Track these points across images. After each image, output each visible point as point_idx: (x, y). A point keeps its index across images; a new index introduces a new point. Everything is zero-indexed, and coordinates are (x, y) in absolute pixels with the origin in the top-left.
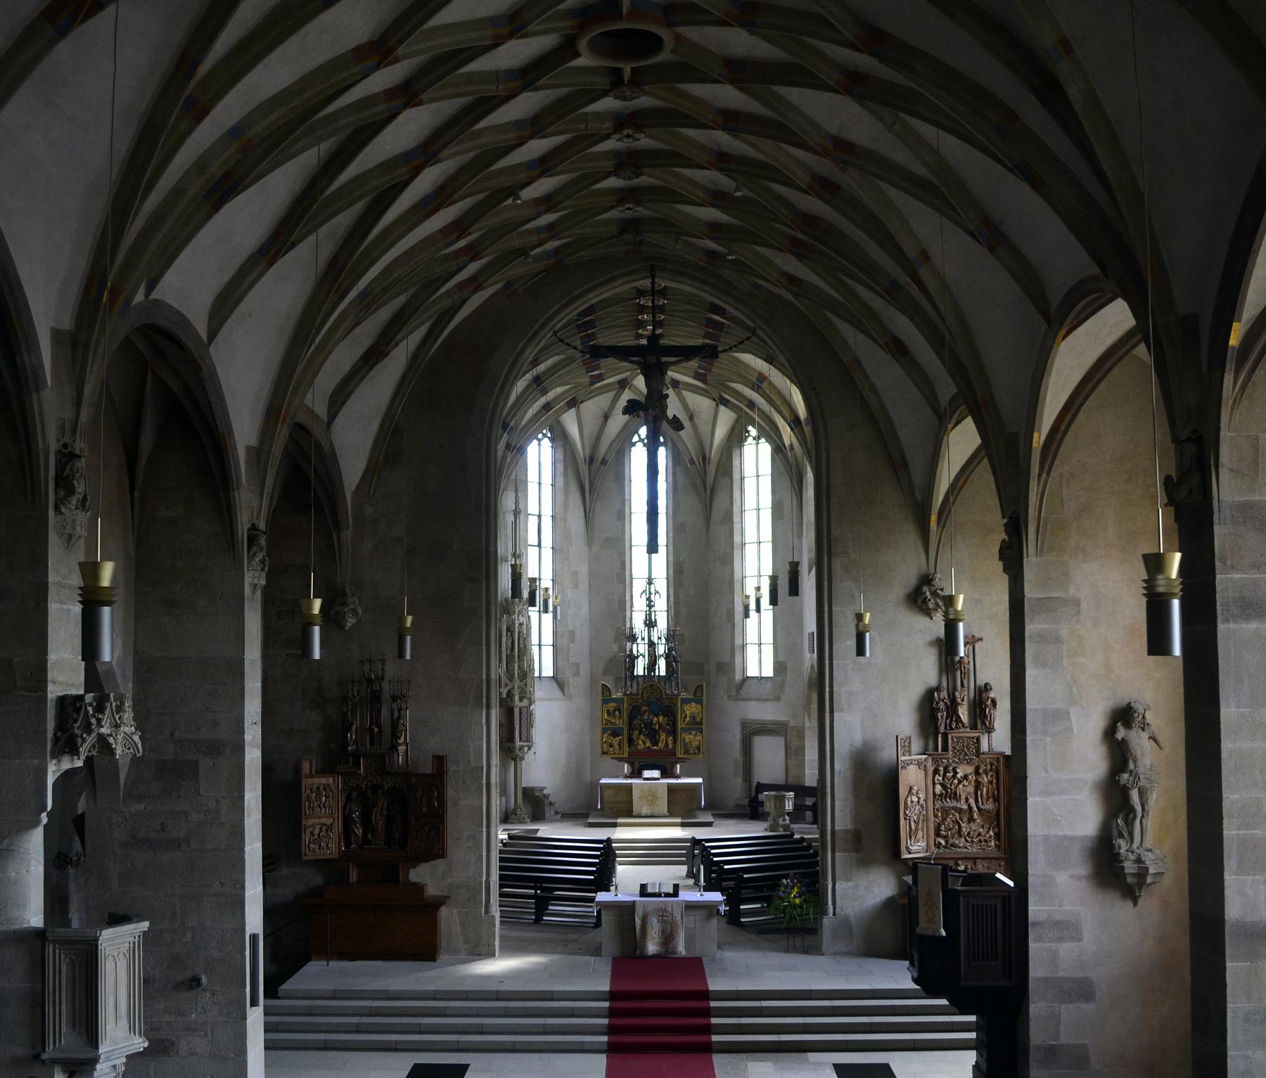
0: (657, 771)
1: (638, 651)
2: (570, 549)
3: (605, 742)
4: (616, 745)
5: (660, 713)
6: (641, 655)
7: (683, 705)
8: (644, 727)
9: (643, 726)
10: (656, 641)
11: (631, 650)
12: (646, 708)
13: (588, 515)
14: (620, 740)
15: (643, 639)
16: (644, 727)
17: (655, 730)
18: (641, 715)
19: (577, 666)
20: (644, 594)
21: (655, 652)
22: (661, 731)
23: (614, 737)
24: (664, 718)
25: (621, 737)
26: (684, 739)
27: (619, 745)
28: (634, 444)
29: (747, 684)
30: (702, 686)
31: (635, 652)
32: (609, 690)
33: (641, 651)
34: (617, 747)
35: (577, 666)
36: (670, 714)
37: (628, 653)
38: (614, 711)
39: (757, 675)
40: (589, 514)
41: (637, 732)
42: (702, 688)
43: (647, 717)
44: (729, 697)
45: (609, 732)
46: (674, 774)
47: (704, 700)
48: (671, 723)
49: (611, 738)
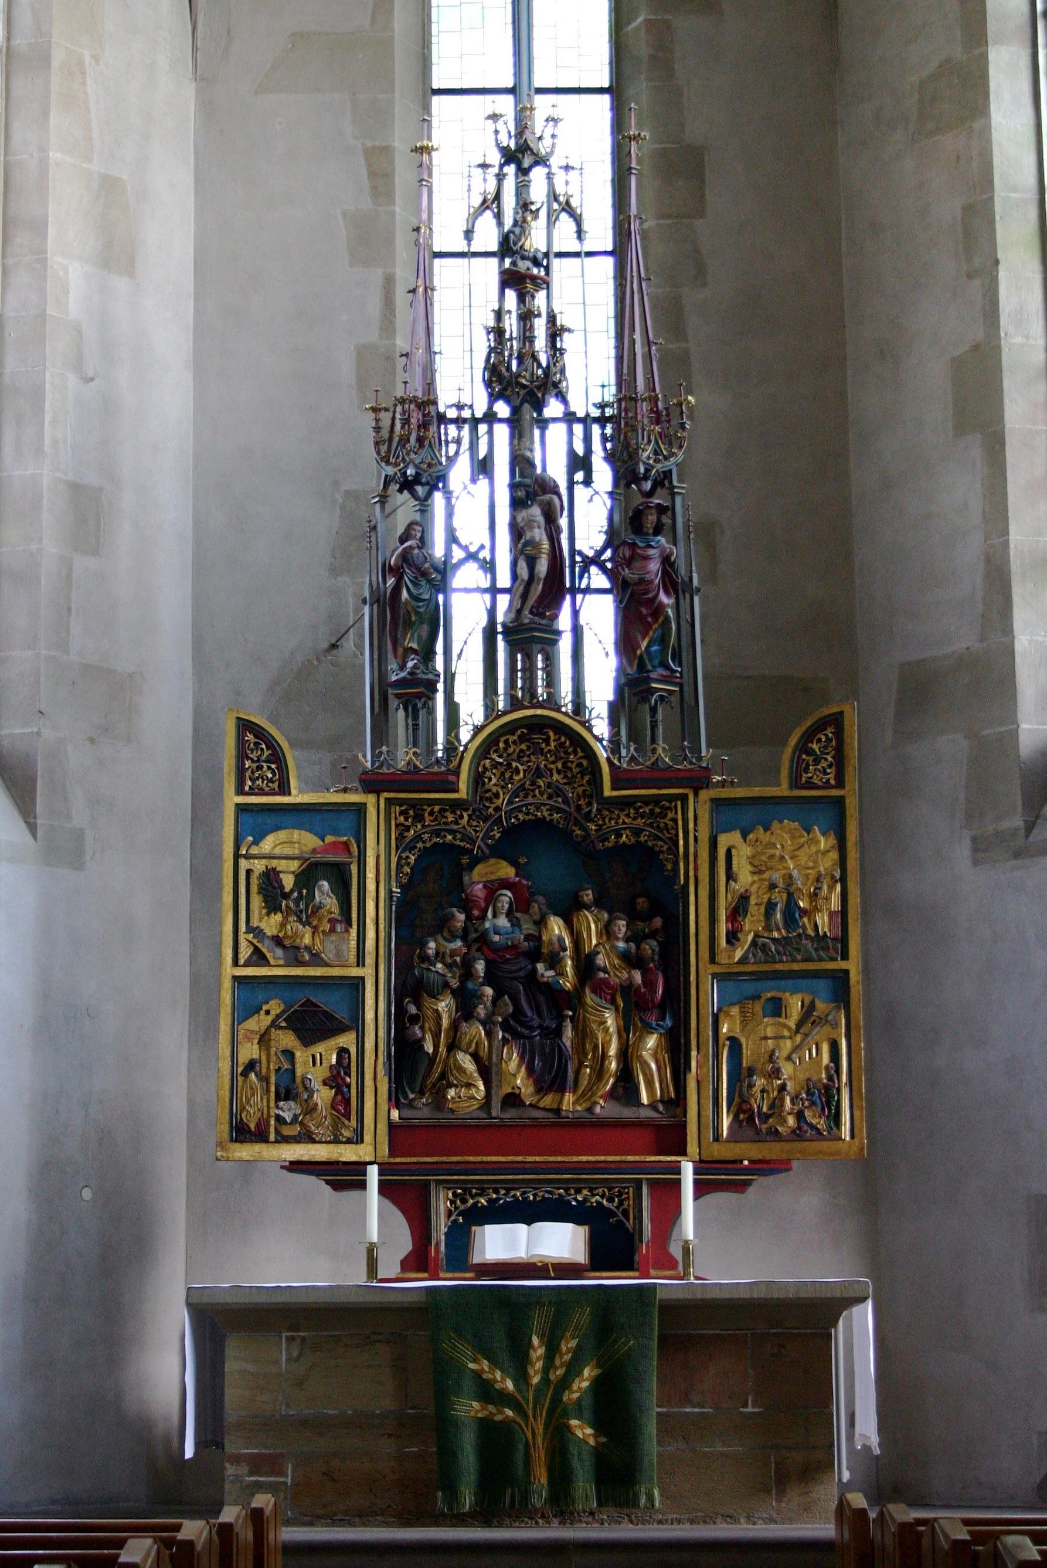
0: (570, 1226)
1: (452, 538)
3: (251, 1066)
4: (316, 1085)
5: (588, 896)
6: (472, 556)
7: (724, 840)
8: (489, 980)
9: (480, 966)
10: (557, 470)
12: (507, 871)
14: (343, 1052)
16: (489, 980)
17: (552, 991)
18: (466, 909)
20: (488, 214)
22: (590, 998)
23: (308, 1039)
24: (607, 932)
25: (347, 1040)
26: (735, 1044)
27: (336, 1080)
30: (836, 721)
32: (277, 758)
34: (323, 1096)
36: (642, 903)
38: (307, 877)
41: (445, 1006)
42: (839, 733)
43: (503, 922)
45: (275, 1007)
47: (852, 805)
48: (650, 947)
49: (286, 1039)
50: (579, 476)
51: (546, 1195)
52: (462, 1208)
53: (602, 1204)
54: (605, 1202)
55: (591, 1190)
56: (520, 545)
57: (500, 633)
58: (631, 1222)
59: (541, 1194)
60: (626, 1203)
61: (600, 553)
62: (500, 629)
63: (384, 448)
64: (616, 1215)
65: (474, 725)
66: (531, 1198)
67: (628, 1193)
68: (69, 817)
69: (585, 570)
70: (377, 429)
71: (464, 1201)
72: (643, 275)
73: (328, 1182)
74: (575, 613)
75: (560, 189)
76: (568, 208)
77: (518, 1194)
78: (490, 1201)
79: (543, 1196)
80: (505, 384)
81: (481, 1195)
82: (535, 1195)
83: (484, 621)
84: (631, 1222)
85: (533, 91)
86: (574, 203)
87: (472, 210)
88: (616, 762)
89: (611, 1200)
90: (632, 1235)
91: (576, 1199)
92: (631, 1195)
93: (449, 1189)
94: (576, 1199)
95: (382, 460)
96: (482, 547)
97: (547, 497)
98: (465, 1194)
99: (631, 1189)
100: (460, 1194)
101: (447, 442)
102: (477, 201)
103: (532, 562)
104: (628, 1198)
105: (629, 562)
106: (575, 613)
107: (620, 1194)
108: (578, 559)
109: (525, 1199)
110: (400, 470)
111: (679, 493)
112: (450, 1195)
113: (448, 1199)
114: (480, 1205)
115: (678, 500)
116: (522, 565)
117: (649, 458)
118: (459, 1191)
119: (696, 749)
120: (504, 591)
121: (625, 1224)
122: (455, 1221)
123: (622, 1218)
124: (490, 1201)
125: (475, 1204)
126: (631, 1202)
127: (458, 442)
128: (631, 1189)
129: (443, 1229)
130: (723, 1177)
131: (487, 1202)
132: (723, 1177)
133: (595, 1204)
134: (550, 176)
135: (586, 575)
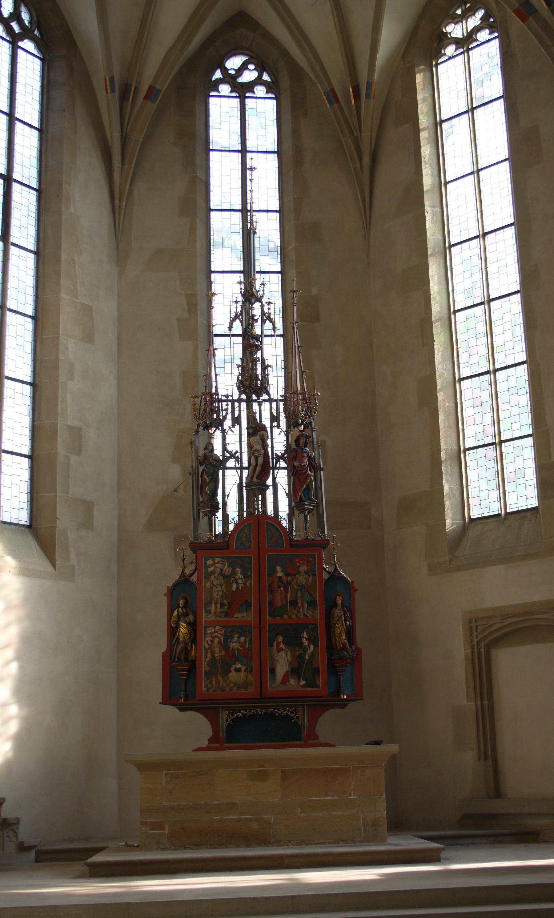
2: (76, 258)
10: (266, 422)
11: (209, 447)
13: (117, 202)
15: (236, 421)
19: (88, 506)
20: (238, 321)
21: (265, 446)
28: (215, 86)
29: (471, 534)
31: (218, 451)
33: (233, 447)
35: (88, 506)
37: (201, 453)
39: (495, 509)
40: (120, 201)
44: (433, 569)
46: (317, 738)
50: (275, 424)
51: (266, 712)
52: (232, 717)
53: (288, 714)
54: (289, 713)
55: (284, 709)
56: (252, 452)
57: (245, 486)
58: (300, 721)
59: (263, 711)
60: (298, 714)
61: (283, 454)
62: (244, 485)
63: (197, 413)
64: (294, 719)
65: (235, 523)
66: (260, 713)
67: (299, 710)
68: (69, 561)
69: (278, 461)
70: (194, 405)
71: (233, 715)
72: (299, 345)
73: (178, 708)
74: (274, 479)
75: (266, 311)
76: (269, 318)
77: (255, 711)
78: (243, 714)
79: (265, 712)
80: (245, 387)
81: (239, 712)
82: (262, 712)
83: (238, 482)
84: (300, 721)
85: (255, 272)
86: (272, 316)
87: (231, 319)
88: (291, 537)
89: (292, 713)
90: (300, 727)
91: (278, 713)
92: (300, 710)
93: (227, 710)
94: (278, 713)
95: (196, 418)
96: (237, 452)
97: (262, 432)
98: (233, 712)
99: (300, 708)
100: (231, 712)
101: (222, 410)
102: (233, 315)
103: (256, 458)
104: (299, 712)
105: (295, 459)
106: (274, 479)
107: (295, 710)
108: (275, 457)
109: (258, 713)
110: (204, 422)
111: (315, 431)
112: (227, 712)
113: (227, 714)
114: (239, 716)
115: (314, 433)
116: (253, 459)
117: (303, 417)
118: (231, 711)
119: (323, 532)
120: (245, 468)
121: (298, 722)
122: (229, 723)
123: (296, 720)
124: (243, 714)
125: (237, 716)
126: (300, 714)
127: (227, 410)
128: (300, 708)
129: (225, 727)
130: (337, 703)
131: (242, 715)
132: (337, 703)
133: (286, 715)
134: (262, 306)
135: (278, 463)
